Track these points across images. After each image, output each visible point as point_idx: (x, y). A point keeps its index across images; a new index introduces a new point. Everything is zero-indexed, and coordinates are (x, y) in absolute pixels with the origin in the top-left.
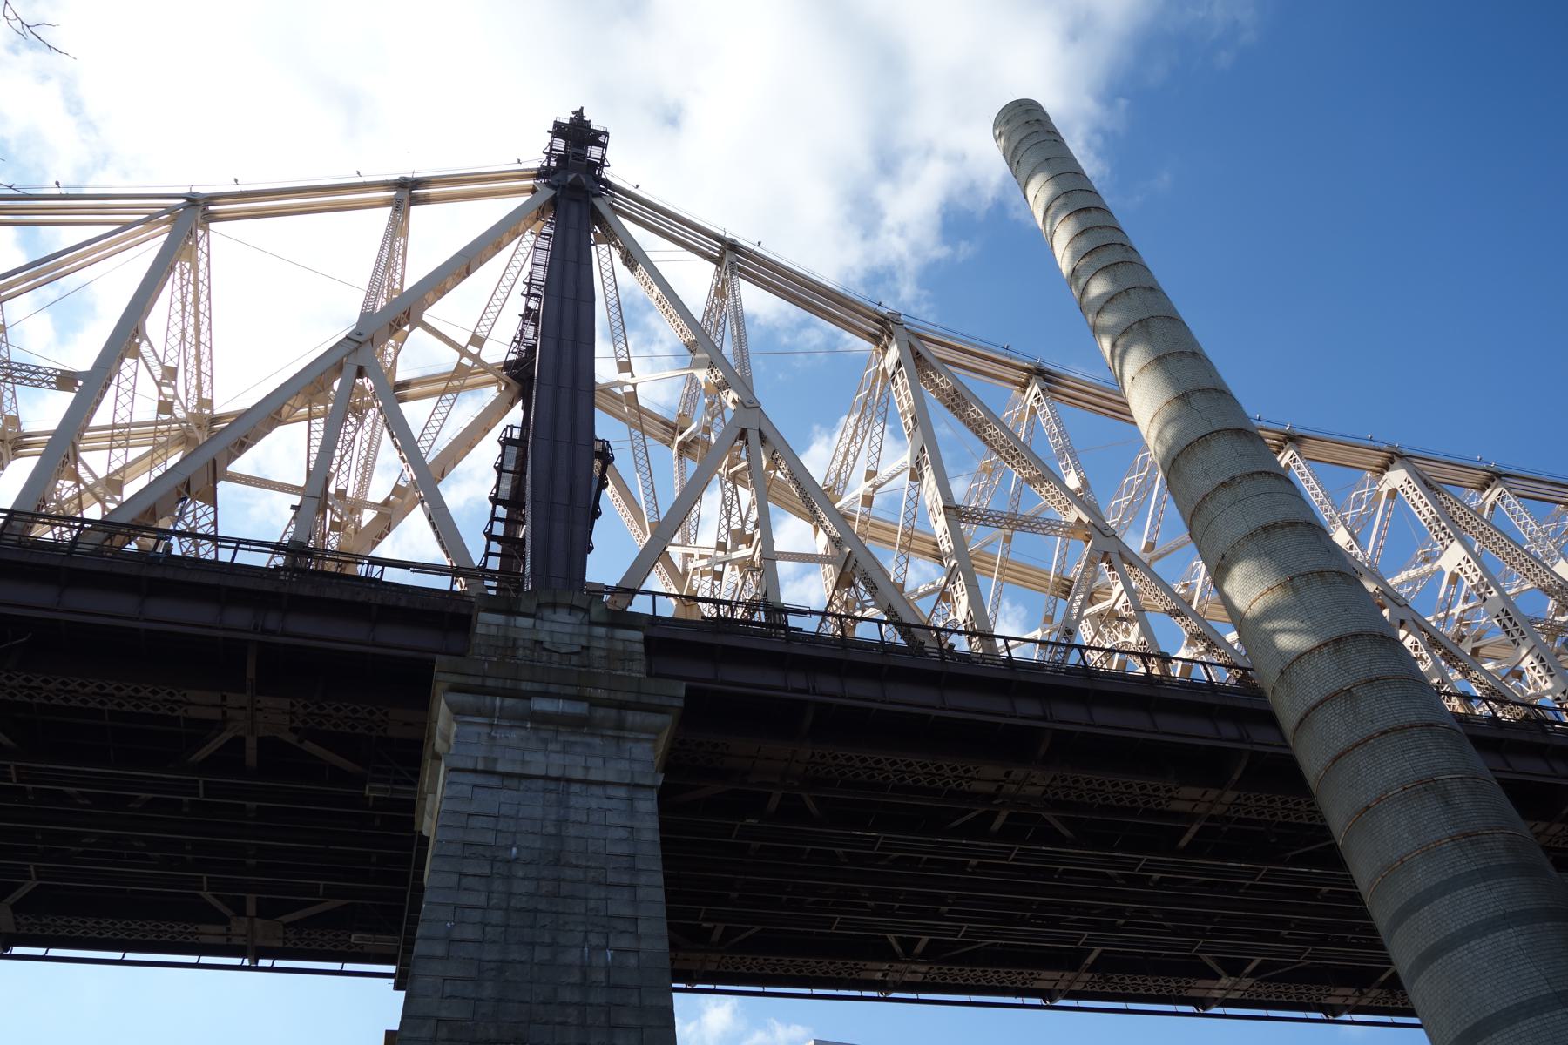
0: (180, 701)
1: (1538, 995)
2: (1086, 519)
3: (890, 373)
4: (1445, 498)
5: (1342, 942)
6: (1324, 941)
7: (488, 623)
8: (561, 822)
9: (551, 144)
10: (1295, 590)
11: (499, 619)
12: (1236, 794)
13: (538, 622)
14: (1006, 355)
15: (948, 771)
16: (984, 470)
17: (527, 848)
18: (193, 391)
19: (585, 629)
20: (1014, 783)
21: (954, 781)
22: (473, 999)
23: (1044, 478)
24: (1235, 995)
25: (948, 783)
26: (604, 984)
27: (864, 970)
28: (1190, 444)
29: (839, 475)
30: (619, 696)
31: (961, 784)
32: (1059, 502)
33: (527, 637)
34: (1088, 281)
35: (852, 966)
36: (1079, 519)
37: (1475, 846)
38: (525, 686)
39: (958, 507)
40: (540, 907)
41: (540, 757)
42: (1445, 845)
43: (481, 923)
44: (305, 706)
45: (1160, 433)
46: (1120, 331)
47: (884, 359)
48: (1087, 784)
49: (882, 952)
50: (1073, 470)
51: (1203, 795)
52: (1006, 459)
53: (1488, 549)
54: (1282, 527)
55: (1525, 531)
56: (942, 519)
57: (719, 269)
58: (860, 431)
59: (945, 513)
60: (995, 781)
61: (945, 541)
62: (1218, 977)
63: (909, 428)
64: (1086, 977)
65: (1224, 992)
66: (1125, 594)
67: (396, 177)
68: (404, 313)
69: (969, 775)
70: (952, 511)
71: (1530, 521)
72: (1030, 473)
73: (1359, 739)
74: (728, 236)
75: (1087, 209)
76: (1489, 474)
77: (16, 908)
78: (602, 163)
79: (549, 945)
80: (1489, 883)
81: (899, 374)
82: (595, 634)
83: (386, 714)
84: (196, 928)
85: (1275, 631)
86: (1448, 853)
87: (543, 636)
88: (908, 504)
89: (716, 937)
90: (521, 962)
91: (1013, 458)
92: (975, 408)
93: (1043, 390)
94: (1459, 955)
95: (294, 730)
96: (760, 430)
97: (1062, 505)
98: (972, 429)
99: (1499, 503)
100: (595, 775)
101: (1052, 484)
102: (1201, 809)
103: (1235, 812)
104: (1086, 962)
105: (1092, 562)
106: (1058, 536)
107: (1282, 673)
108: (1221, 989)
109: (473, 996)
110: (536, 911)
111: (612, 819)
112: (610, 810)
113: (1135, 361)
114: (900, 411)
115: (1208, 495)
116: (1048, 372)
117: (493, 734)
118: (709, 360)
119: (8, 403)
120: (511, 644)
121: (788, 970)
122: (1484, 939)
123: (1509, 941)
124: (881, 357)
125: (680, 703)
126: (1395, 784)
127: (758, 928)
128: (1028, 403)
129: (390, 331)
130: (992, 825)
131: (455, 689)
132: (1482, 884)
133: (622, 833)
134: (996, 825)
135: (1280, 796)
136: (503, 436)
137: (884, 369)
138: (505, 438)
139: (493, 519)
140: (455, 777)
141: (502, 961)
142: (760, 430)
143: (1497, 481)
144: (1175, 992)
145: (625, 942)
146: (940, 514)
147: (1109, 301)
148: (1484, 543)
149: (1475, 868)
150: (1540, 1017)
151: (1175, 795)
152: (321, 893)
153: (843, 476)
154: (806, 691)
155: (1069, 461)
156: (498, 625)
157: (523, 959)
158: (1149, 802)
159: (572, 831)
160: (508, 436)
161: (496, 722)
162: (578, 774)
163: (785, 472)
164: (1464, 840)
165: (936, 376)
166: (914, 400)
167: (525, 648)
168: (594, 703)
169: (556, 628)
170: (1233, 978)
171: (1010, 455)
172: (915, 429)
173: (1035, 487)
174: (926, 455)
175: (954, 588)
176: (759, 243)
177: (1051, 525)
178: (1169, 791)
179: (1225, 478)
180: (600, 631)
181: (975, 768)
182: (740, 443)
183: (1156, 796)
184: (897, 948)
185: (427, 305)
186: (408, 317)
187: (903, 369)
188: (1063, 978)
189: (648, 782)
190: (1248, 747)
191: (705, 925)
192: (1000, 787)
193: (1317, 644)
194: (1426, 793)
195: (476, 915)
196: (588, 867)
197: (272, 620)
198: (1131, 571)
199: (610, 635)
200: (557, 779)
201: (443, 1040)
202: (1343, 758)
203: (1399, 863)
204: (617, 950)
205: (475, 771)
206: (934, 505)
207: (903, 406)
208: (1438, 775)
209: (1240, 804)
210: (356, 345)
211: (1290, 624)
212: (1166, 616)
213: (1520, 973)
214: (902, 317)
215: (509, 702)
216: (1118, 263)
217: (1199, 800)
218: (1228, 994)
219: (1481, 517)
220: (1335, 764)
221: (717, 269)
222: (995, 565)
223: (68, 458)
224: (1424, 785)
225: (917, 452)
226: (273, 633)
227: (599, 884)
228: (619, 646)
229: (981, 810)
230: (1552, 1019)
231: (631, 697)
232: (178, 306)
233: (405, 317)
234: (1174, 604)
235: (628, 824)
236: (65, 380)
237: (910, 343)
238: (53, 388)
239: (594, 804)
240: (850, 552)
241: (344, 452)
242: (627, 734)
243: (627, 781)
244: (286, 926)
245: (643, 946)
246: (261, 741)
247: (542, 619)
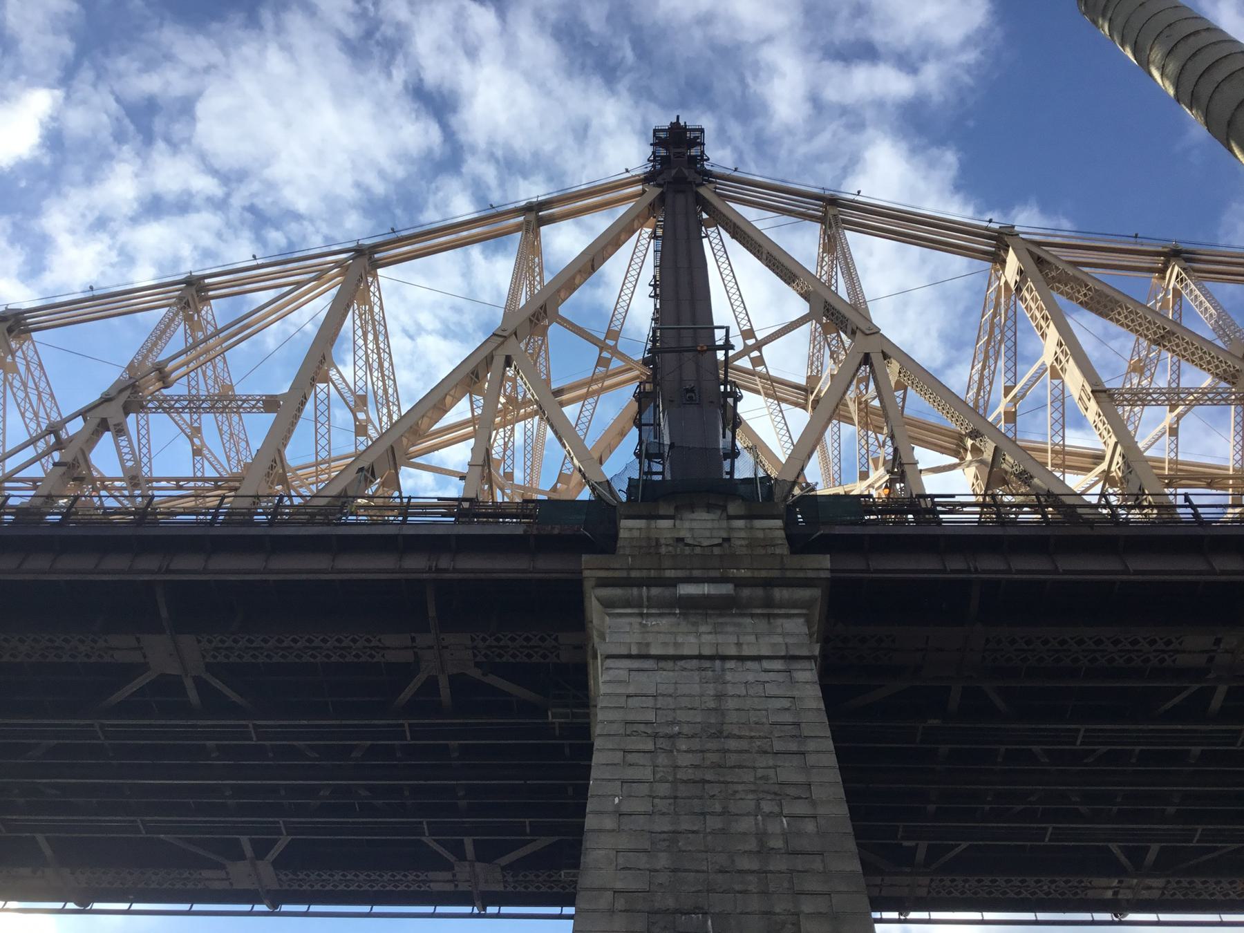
0: (378, 647)
7: (629, 528)
8: (720, 697)
9: (654, 153)
11: (641, 523)
13: (678, 522)
14: (1136, 243)
17: (688, 722)
18: (385, 419)
19: (724, 524)
22: (648, 870)
26: (783, 851)
27: (1089, 888)
30: (764, 574)
33: (669, 536)
35: (1076, 884)
38: (670, 574)
39: (1109, 390)
40: (708, 777)
41: (692, 639)
43: (650, 796)
44: (484, 640)
47: (1004, 273)
49: (1111, 867)
56: (1093, 405)
60: (1206, 652)
68: (541, 308)
69: (1171, 647)
70: (1103, 395)
77: (277, 864)
78: (702, 158)
79: (720, 815)
82: (734, 527)
83: (556, 639)
84: (427, 876)
87: (682, 534)
89: (921, 855)
90: (693, 832)
93: (1184, 269)
95: (478, 665)
96: (883, 352)
100: (746, 651)
106: (1230, 404)
109: (648, 866)
110: (704, 782)
111: (771, 690)
112: (768, 682)
116: (1187, 252)
117: (644, 622)
119: (244, 453)
120: (654, 544)
121: (1005, 893)
127: (964, 845)
128: (1171, 287)
129: (531, 327)
131: (603, 583)
137: (1006, 282)
140: (609, 663)
141: (674, 832)
145: (801, 808)
146: (1089, 400)
152: (528, 830)
153: (981, 402)
154: (969, 571)
156: (640, 529)
157: (695, 828)
159: (731, 704)
162: (733, 651)
167: (667, 545)
168: (739, 583)
169: (695, 525)
176: (859, 192)
180: (740, 523)
181: (1177, 639)
182: (864, 370)
184: (1123, 859)
185: (560, 300)
186: (545, 312)
189: (805, 652)
191: (906, 843)
192: (1211, 659)
195: (644, 789)
196: (752, 737)
197: (444, 563)
199: (749, 526)
200: (711, 658)
201: (621, 911)
204: (790, 817)
205: (629, 656)
210: (501, 339)
214: (1016, 228)
215: (655, 591)
223: (275, 463)
226: (446, 571)
227: (766, 752)
228: (760, 535)
229: (1196, 686)
231: (776, 574)
233: (542, 312)
235: (789, 694)
236: (270, 403)
237: (1028, 250)
238: (262, 412)
239: (750, 677)
241: (506, 439)
243: (783, 653)
244: (503, 868)
245: (821, 810)
246: (452, 679)
247: (681, 519)
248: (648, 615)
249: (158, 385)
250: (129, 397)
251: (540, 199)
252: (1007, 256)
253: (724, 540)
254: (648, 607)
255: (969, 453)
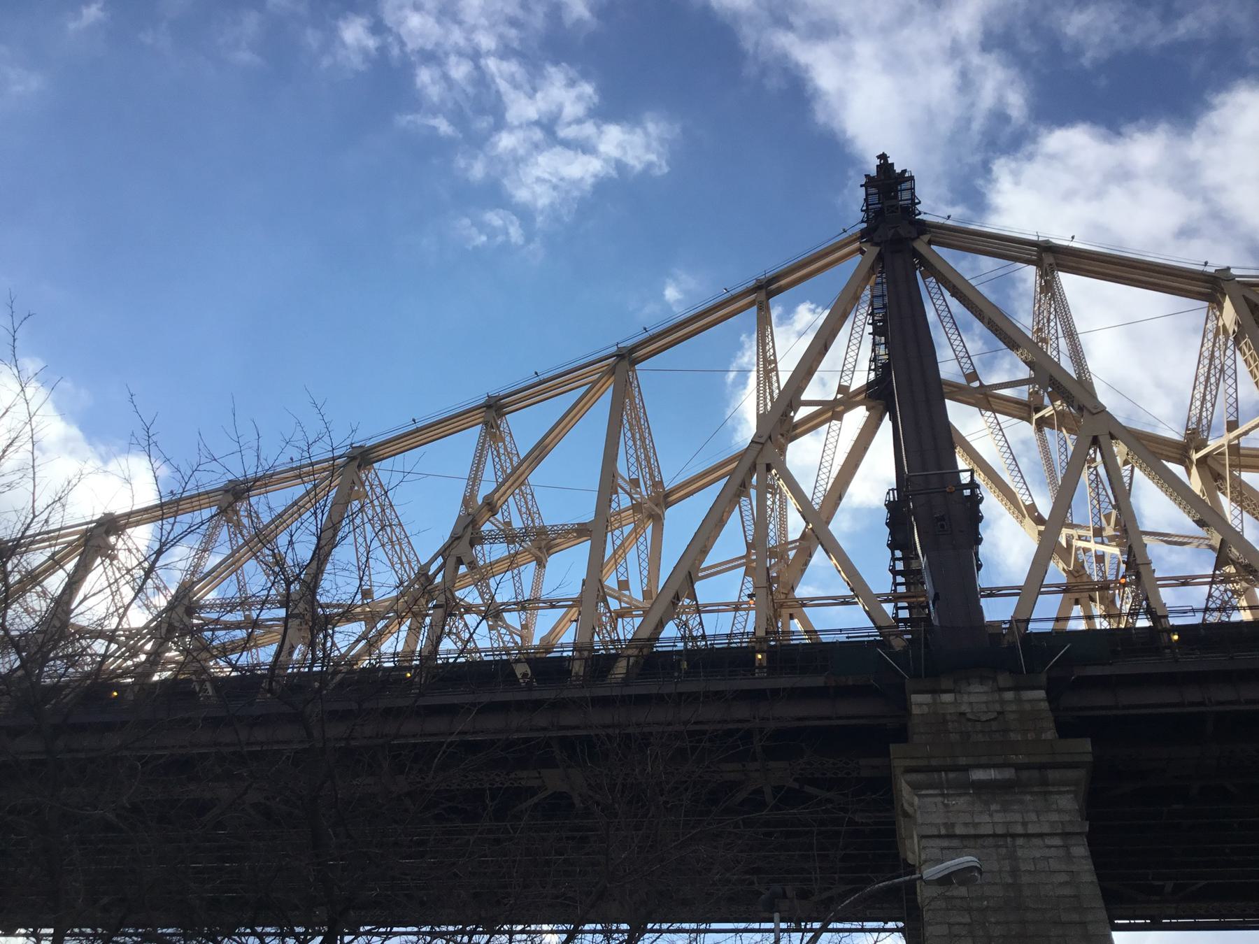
19: (996, 697)
29: (1200, 420)
33: (953, 711)
38: (963, 761)
41: (986, 818)
58: (1213, 380)
67: (752, 284)
74: (1041, 239)
95: (796, 780)
96: (1110, 433)
100: (1032, 829)
111: (1054, 865)
117: (946, 802)
125: (1089, 758)
133: (1063, 878)
136: (888, 499)
137: (1224, 326)
138: (889, 501)
139: (894, 559)
140: (924, 842)
153: (1204, 422)
160: (892, 499)
161: (946, 792)
162: (1019, 829)
168: (1018, 767)
169: (973, 699)
180: (1009, 695)
205: (939, 836)
210: (760, 446)
215: (952, 775)
228: (1027, 707)
232: (630, 443)
239: (1037, 854)
242: (1051, 789)
243: (1059, 831)
247: (960, 692)
248: (948, 795)
249: (490, 513)
250: (472, 534)
251: (767, 275)
252: (1224, 302)
253: (999, 713)
254: (947, 789)
255: (1194, 467)
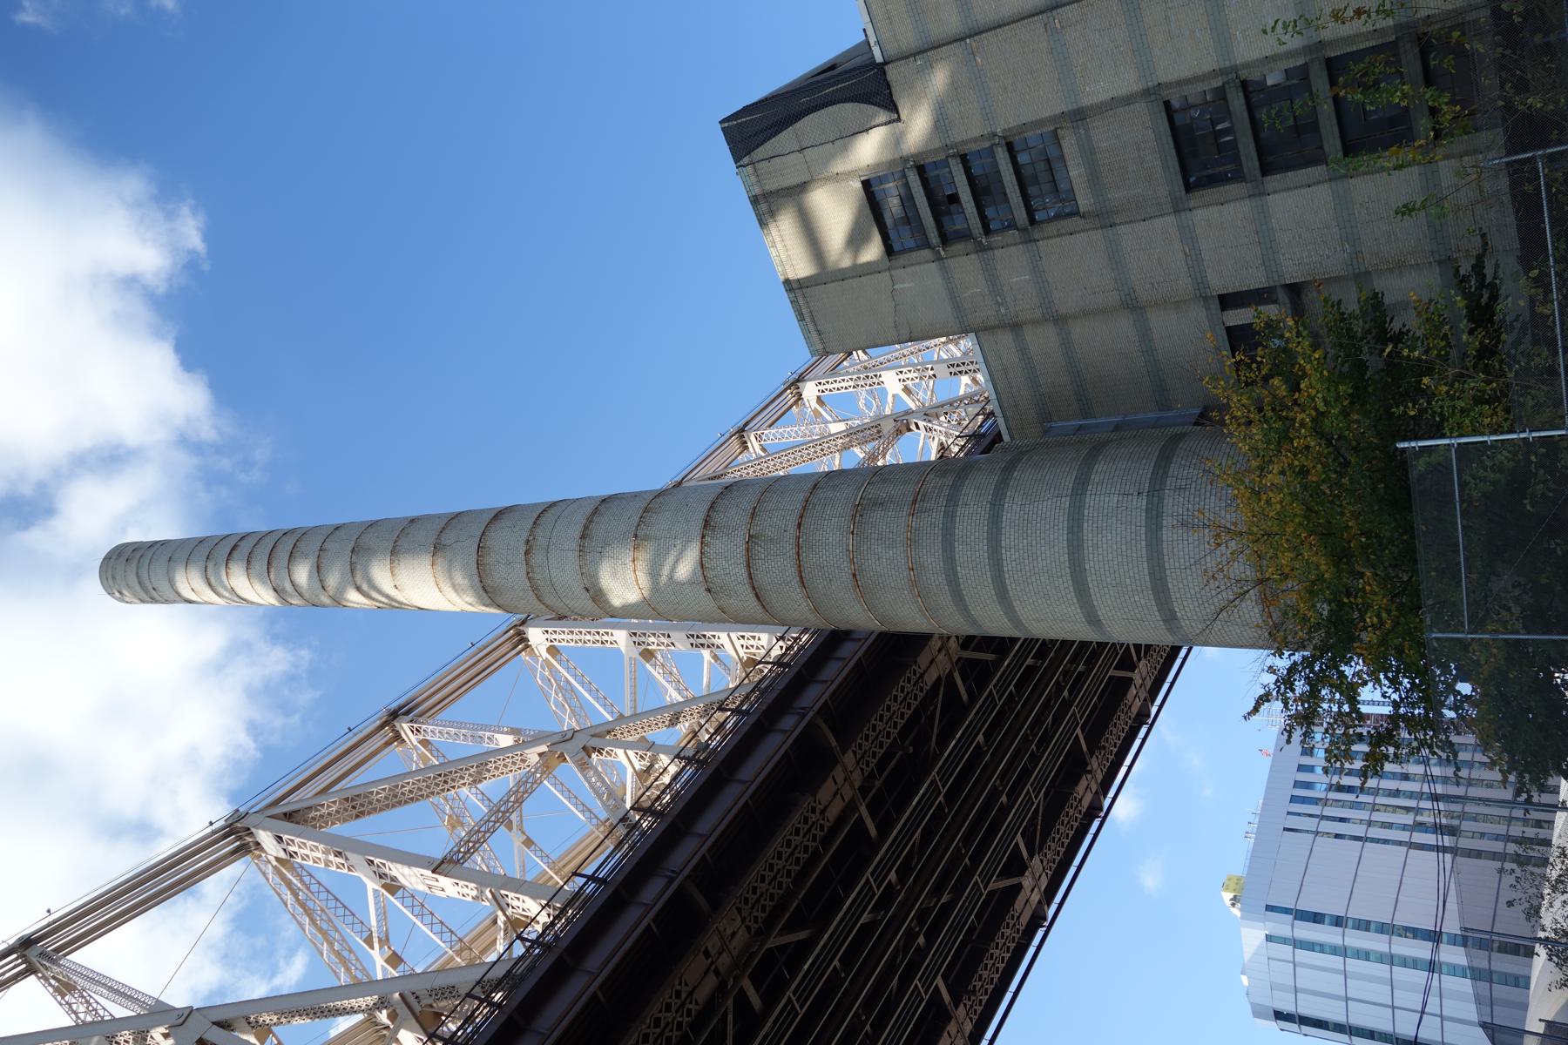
1: (1067, 511)
2: (543, 748)
3: (282, 855)
4: (732, 473)
5: (1035, 758)
6: (1026, 773)
10: (646, 538)
12: (850, 754)
15: (666, 1014)
16: (454, 827)
20: (720, 954)
21: (682, 1016)
23: (482, 764)
24: (1044, 882)
25: (680, 1024)
28: (478, 564)
31: (689, 1011)
32: (514, 763)
34: (291, 582)
36: (540, 755)
37: (926, 499)
42: (914, 523)
45: (454, 587)
46: (350, 574)
47: (267, 853)
48: (763, 880)
50: (496, 736)
51: (836, 783)
52: (443, 790)
53: (790, 468)
54: (591, 521)
55: (794, 437)
56: (445, 882)
57: (40, 975)
59: (440, 874)
60: (706, 972)
61: (465, 891)
62: (1019, 887)
63: (343, 865)
64: (961, 1012)
65: (1036, 890)
66: (629, 752)
69: (684, 996)
71: (789, 429)
72: (470, 775)
73: (794, 551)
74: (11, 942)
75: (235, 547)
76: (737, 436)
80: (960, 503)
81: (288, 844)
85: (671, 577)
86: (921, 523)
88: (416, 913)
91: (446, 782)
92: (375, 790)
94: (1009, 560)
96: (214, 1023)
97: (518, 762)
98: (394, 806)
99: (762, 443)
101: (493, 760)
102: (848, 793)
103: (868, 765)
104: (947, 1003)
105: (584, 766)
106: (542, 782)
107: (709, 590)
108: (1032, 890)
113: (381, 574)
114: (322, 866)
115: (528, 573)
118: (104, 1038)
122: (1003, 530)
123: (1014, 511)
124: (263, 855)
126: (845, 539)
128: (415, 743)
130: (753, 1007)
132: (959, 509)
134: (756, 1002)
135: (873, 719)
137: (277, 859)
142: (214, 1023)
143: (745, 434)
144: (1017, 936)
147: (318, 570)
148: (783, 468)
149: (943, 508)
150: (1085, 518)
151: (822, 807)
155: (487, 734)
158: (814, 835)
163: (275, 1020)
164: (917, 506)
165: (319, 810)
166: (320, 843)
170: (1027, 874)
171: (442, 784)
172: (347, 859)
173: (485, 778)
174: (377, 861)
175: (513, 907)
176: (49, 911)
177: (526, 782)
178: (814, 810)
179: (523, 548)
181: (680, 984)
183: (812, 826)
187: (285, 837)
188: (952, 1035)
190: (811, 714)
192: (717, 972)
193: (699, 544)
194: (864, 517)
198: (615, 735)
202: (803, 574)
203: (912, 573)
206: (428, 882)
207: (320, 859)
208: (855, 500)
209: (862, 757)
211: (671, 559)
212: (671, 728)
213: (1044, 515)
214: (241, 810)
216: (295, 544)
217: (838, 789)
218: (1039, 889)
219: (762, 457)
220: (806, 585)
221: (39, 978)
222: (552, 877)
224: (858, 515)
225: (369, 870)
229: (730, 1002)
230: (1091, 509)
234: (667, 715)
240: (400, 994)
